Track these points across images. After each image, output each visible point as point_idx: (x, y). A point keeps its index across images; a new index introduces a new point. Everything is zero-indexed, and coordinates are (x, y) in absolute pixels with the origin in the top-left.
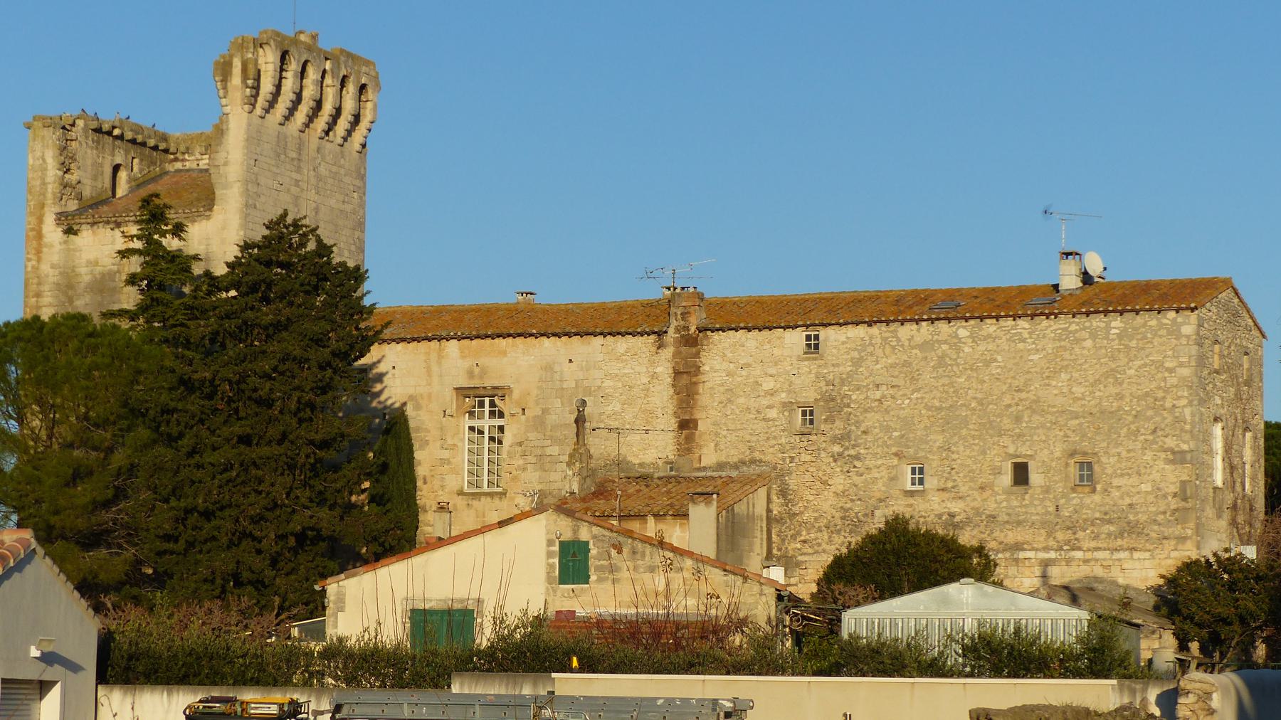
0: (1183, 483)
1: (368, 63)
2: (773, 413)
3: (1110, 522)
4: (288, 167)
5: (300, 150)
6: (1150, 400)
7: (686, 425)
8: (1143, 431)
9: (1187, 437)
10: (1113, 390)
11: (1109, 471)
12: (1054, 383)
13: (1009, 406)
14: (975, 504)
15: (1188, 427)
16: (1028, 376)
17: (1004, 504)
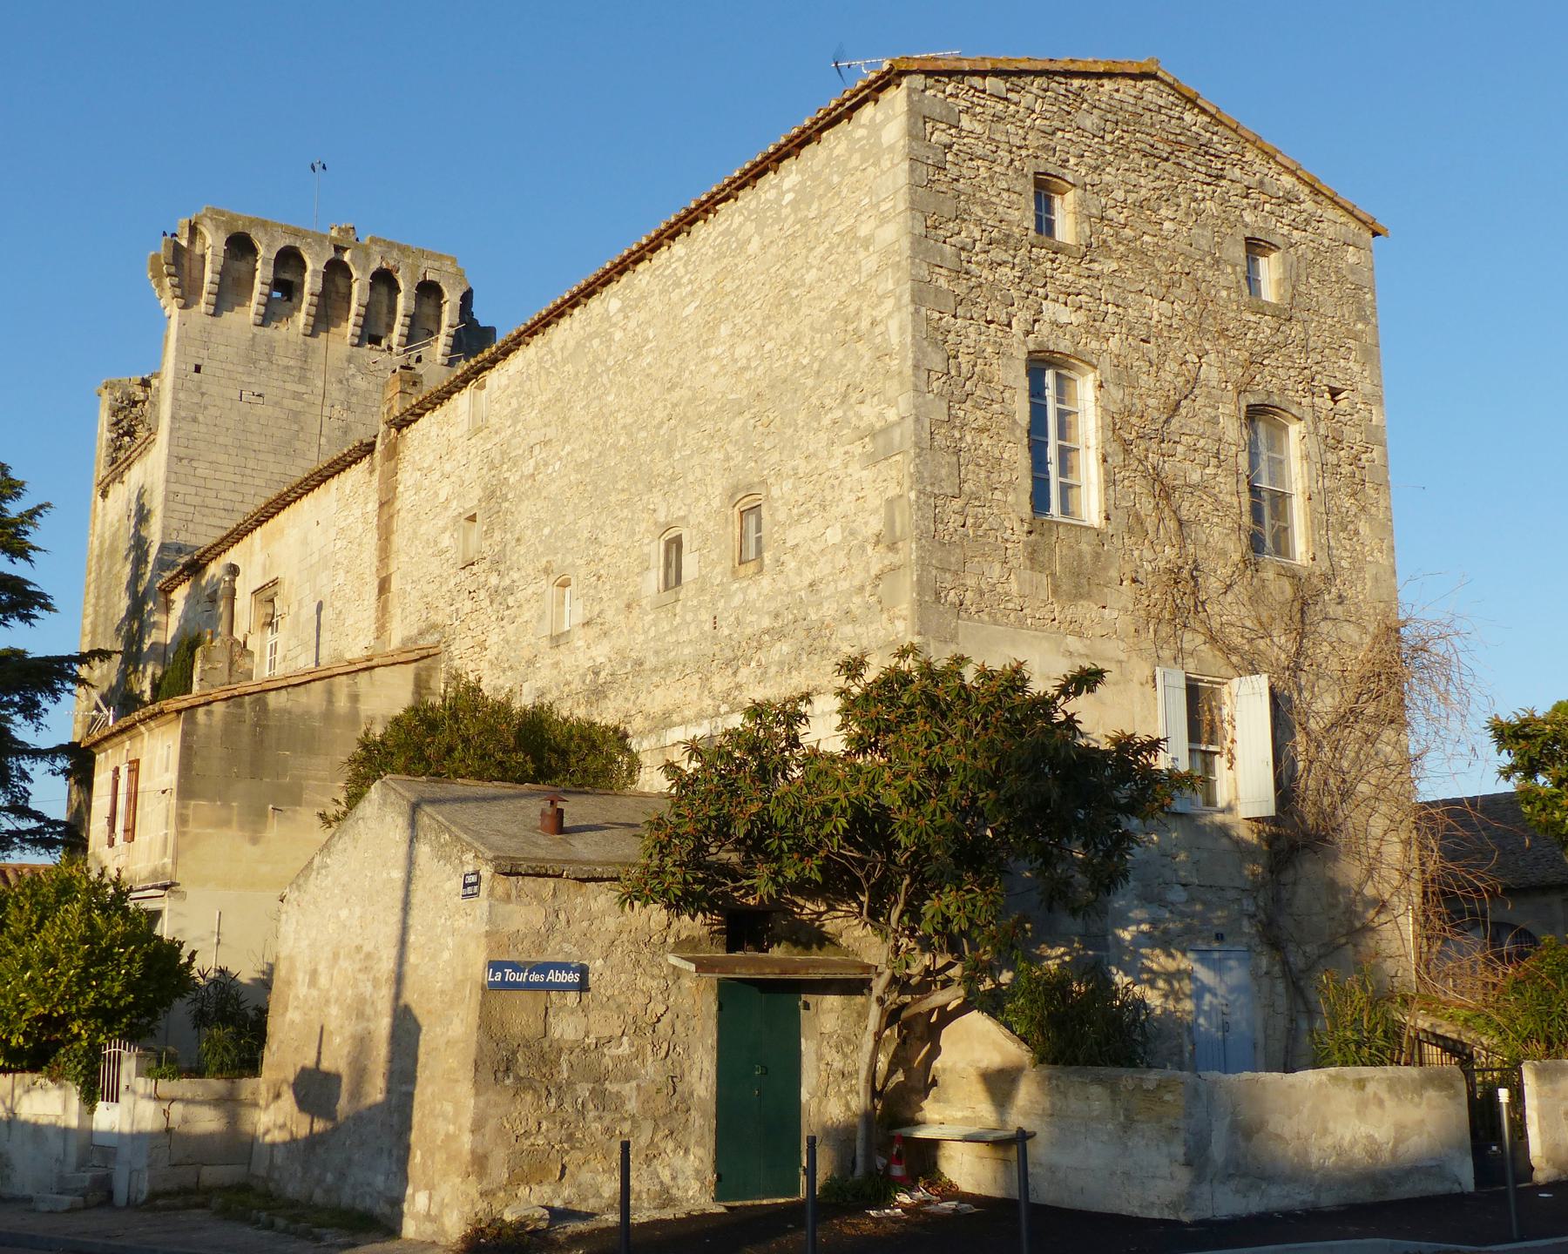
0: (890, 502)
1: (440, 257)
2: (446, 541)
3: (780, 635)
4: (275, 375)
5: (305, 356)
6: (839, 323)
7: (384, 586)
8: (827, 401)
9: (893, 387)
10: (788, 328)
11: (781, 516)
12: (713, 351)
13: (662, 423)
14: (622, 642)
15: (894, 364)
16: (681, 355)
17: (652, 633)
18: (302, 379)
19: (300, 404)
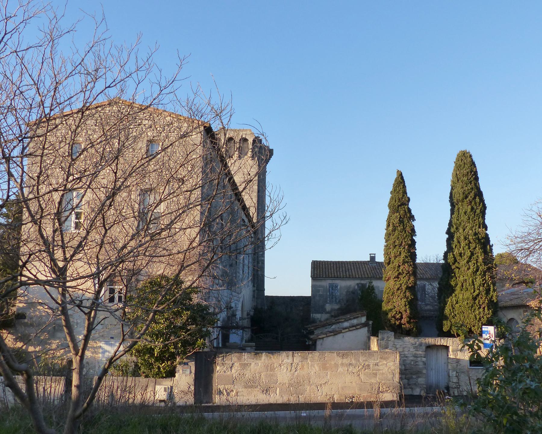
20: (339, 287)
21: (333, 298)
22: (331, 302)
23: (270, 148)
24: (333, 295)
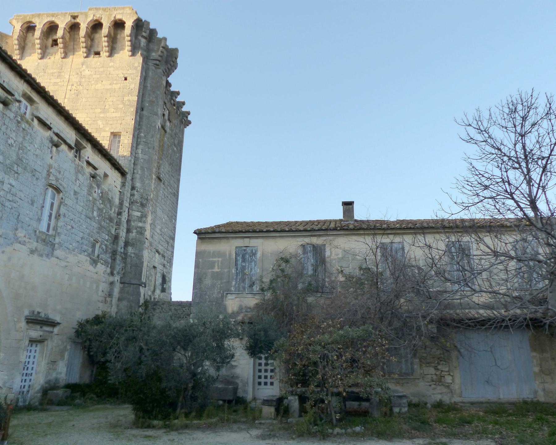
18: (59, 77)
19: (57, 87)
20: (259, 255)
21: (243, 280)
22: (239, 292)
23: (171, 45)
24: (244, 274)
